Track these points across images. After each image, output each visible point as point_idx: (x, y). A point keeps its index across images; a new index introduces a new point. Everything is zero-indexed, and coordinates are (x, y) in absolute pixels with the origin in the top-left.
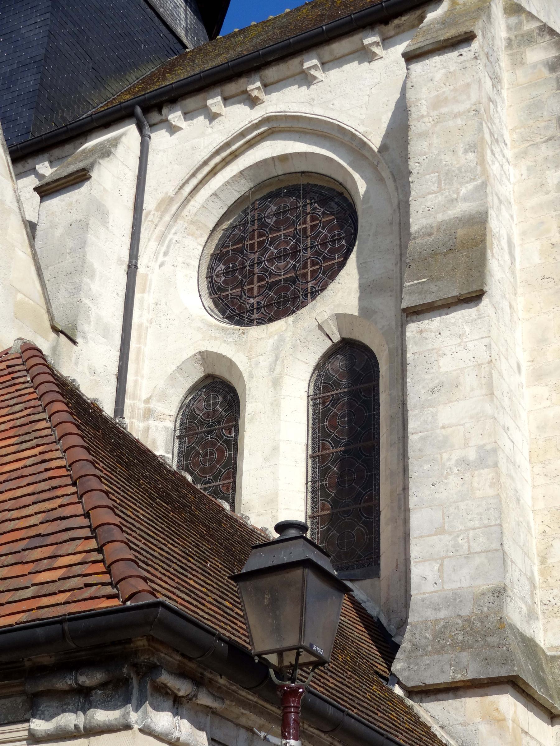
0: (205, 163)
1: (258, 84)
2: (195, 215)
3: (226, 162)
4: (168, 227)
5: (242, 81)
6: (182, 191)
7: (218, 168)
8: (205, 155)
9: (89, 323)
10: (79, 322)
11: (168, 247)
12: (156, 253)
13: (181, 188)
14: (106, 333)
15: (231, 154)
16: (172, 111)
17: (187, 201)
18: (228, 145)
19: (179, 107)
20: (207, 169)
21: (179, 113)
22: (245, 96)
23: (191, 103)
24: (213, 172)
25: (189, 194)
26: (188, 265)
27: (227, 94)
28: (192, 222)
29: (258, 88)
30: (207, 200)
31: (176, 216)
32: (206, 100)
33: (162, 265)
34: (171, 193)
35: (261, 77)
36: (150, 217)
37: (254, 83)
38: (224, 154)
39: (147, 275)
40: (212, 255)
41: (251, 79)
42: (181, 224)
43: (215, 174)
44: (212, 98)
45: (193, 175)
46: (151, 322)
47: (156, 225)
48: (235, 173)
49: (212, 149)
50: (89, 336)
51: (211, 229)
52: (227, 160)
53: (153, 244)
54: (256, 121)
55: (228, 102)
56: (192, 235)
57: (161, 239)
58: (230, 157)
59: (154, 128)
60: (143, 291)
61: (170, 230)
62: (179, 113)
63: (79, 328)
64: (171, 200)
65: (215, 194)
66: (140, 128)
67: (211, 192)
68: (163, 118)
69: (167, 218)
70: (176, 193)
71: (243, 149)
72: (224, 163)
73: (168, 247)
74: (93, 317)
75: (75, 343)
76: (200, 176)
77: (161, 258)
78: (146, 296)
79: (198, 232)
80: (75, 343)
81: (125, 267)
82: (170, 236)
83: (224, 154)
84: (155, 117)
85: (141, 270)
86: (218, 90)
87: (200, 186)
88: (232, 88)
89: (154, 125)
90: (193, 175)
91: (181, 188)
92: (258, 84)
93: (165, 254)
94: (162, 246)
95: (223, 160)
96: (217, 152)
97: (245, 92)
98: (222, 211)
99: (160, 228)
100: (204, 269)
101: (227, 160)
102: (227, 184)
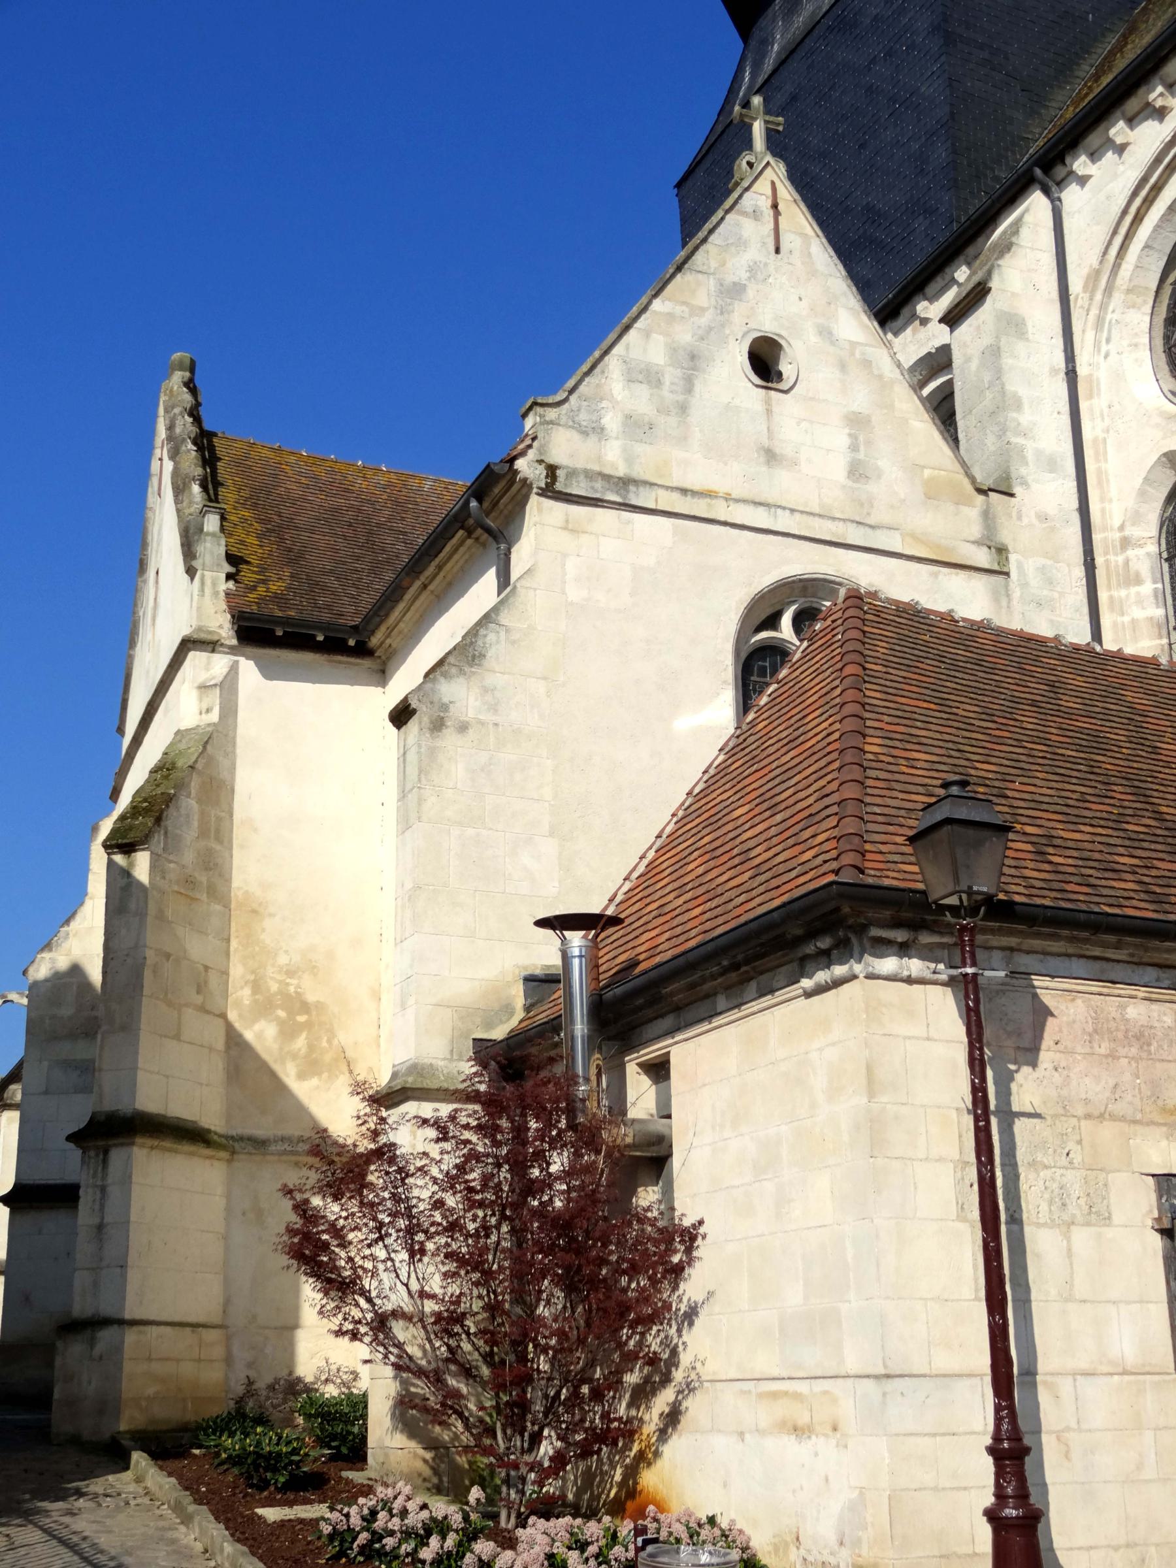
0: (1125, 212)
1: (1160, 89)
2: (1130, 280)
3: (1149, 201)
4: (1103, 307)
5: (1142, 91)
6: (1106, 257)
7: (1142, 211)
8: (1122, 203)
9: (1027, 464)
10: (1012, 469)
11: (1109, 331)
12: (1097, 345)
13: (1105, 253)
14: (1052, 465)
15: (1152, 189)
16: (1076, 158)
17: (1116, 266)
18: (1144, 180)
19: (1082, 151)
20: (1128, 219)
21: (1083, 158)
22: (1149, 110)
23: (1093, 140)
24: (1138, 219)
25: (1117, 257)
26: (1136, 345)
27: (1130, 113)
28: (1129, 291)
29: (1161, 95)
30: (1140, 257)
31: (1109, 290)
32: (1108, 130)
33: (1106, 357)
34: (1095, 264)
35: (1161, 79)
36: (1080, 302)
37: (1154, 90)
38: (1143, 193)
39: (1091, 375)
40: (1166, 320)
41: (1151, 85)
42: (1118, 297)
43: (1142, 220)
44: (1114, 125)
45: (1115, 232)
46: (1108, 431)
47: (1088, 310)
48: (1162, 212)
49: (1128, 193)
50: (1030, 479)
51: (1155, 289)
52: (1150, 198)
53: (1090, 335)
54: (1169, 138)
55: (1135, 122)
56: (1133, 307)
57: (1099, 323)
58: (1153, 193)
59: (1062, 185)
60: (1090, 396)
61: (1106, 308)
62: (1083, 158)
63: (1013, 475)
64: (1097, 273)
65: (1147, 246)
66: (1047, 192)
67: (1141, 245)
68: (1068, 169)
69: (1098, 296)
70: (1101, 262)
71: (1165, 177)
72: (1147, 203)
73: (1109, 331)
74: (1030, 455)
75: (1012, 495)
76: (1123, 230)
77: (1104, 348)
78: (1095, 401)
79: (1139, 300)
80: (1012, 495)
81: (1062, 375)
82: (1109, 317)
83: (1143, 193)
84: (1060, 172)
85: (1082, 370)
86: (1118, 113)
87: (1127, 242)
88: (1132, 105)
89: (1063, 180)
90: (1115, 232)
91: (1105, 253)
92: (1160, 89)
93: (1108, 341)
94: (1102, 330)
95: (1145, 200)
96: (1135, 194)
97: (1148, 104)
98: (1162, 263)
99: (1094, 312)
100: (1159, 342)
101: (1150, 198)
102: (1157, 227)
